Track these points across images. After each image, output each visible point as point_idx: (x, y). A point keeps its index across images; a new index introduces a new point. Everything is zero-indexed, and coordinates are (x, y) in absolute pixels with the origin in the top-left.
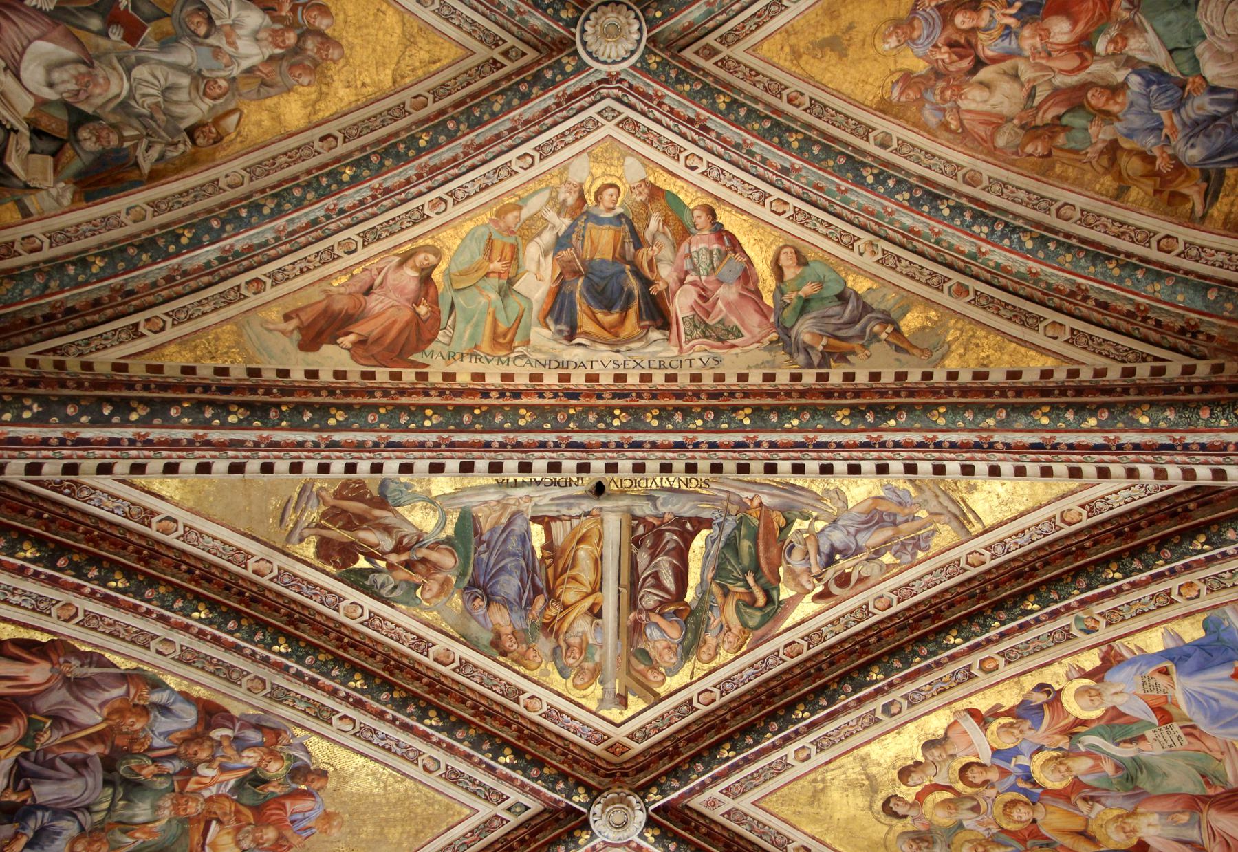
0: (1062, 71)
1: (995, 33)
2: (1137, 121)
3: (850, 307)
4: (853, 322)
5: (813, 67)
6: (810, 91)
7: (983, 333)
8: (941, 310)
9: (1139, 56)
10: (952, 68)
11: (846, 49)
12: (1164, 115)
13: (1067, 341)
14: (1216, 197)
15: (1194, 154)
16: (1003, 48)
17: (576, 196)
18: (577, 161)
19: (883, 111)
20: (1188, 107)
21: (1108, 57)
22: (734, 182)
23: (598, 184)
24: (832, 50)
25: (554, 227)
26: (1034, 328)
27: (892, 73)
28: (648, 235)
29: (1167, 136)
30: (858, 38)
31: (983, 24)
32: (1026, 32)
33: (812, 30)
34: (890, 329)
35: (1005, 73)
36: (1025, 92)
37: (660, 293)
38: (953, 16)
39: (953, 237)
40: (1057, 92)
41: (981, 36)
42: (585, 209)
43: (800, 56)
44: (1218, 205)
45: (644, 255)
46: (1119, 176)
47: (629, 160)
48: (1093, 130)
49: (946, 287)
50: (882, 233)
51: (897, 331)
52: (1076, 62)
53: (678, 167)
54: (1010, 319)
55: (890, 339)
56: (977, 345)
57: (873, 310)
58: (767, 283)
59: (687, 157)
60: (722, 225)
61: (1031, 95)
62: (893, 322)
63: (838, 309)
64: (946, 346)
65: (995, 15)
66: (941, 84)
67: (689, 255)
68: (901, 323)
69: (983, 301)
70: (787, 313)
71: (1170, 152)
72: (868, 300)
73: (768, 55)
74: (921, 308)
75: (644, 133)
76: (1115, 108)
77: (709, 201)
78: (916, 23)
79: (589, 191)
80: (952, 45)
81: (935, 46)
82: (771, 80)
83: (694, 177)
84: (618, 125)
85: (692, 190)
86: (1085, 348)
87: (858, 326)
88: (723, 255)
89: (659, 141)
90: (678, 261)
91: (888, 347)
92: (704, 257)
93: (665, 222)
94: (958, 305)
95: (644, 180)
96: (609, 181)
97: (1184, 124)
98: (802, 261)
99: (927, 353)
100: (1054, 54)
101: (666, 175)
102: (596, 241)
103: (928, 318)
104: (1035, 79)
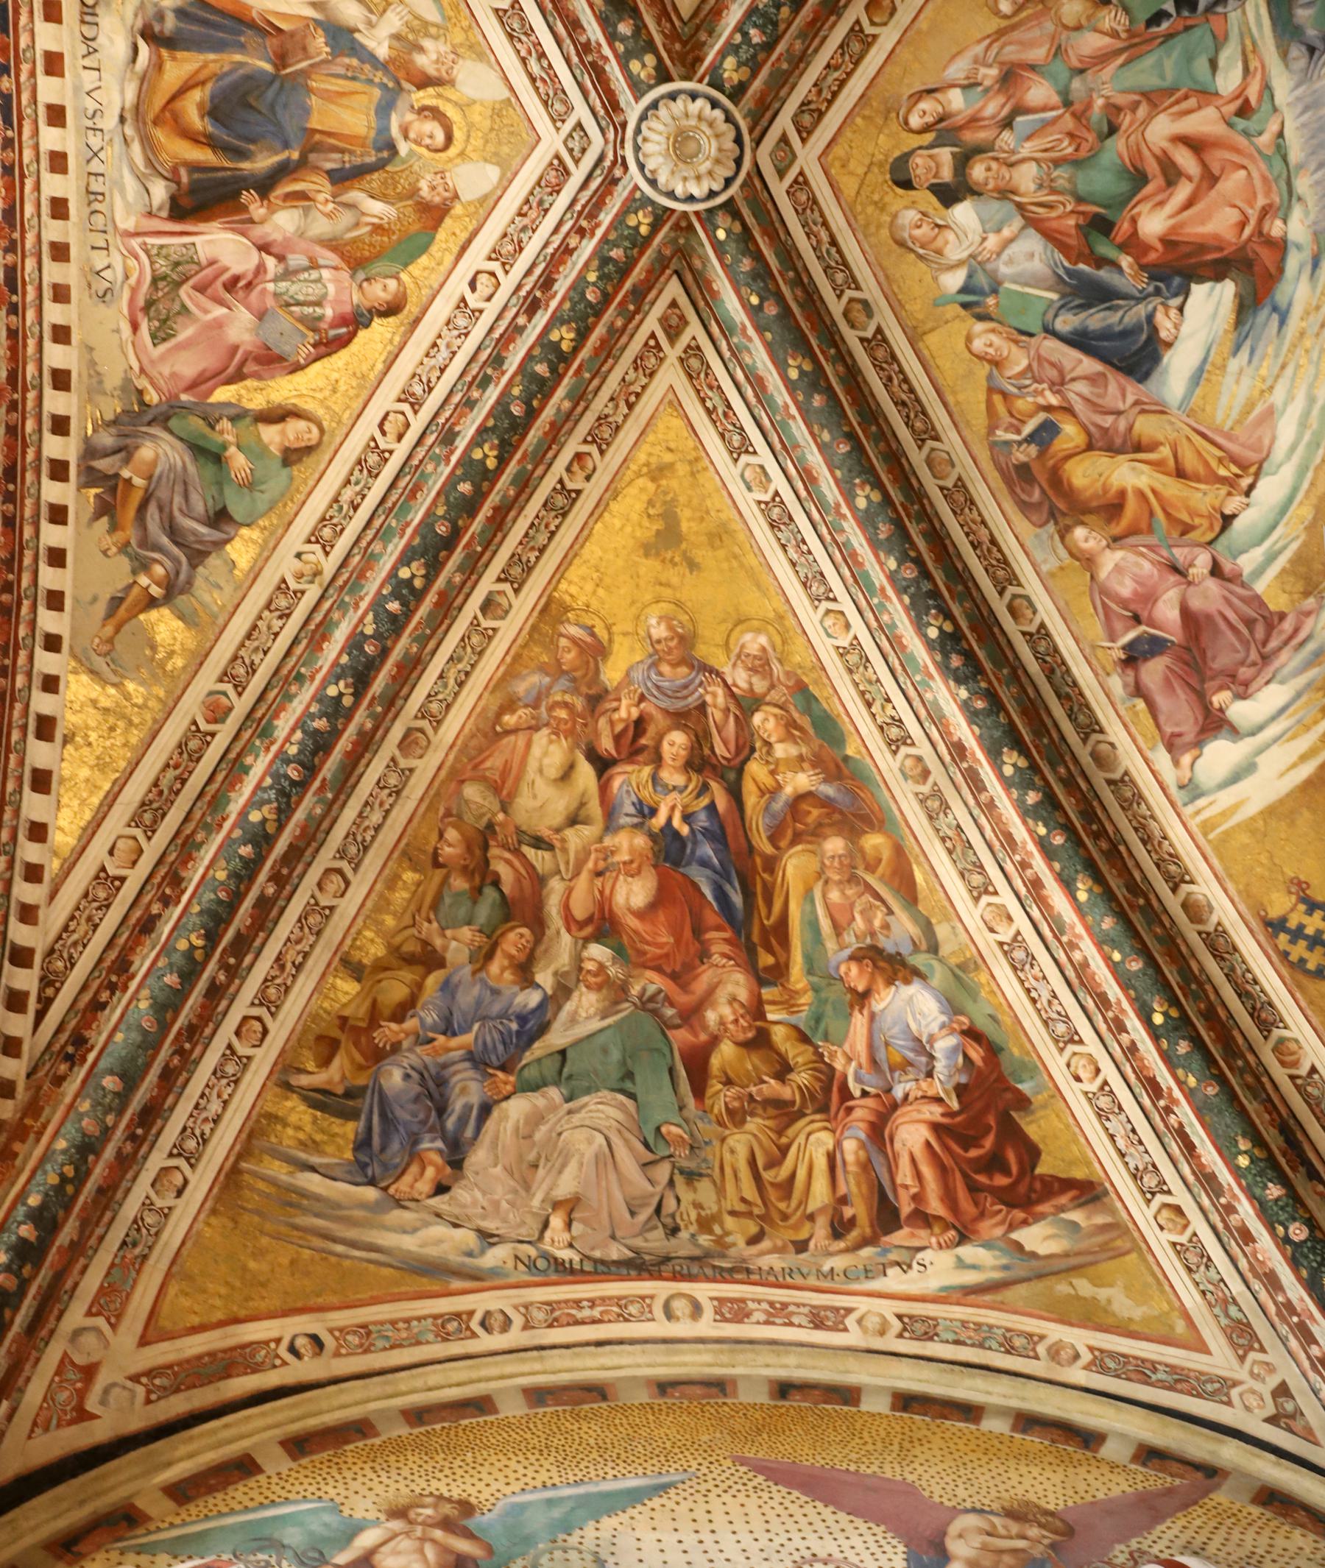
0: (570, 891)
1: (647, 794)
2: (466, 998)
3: (203, 530)
4: (173, 531)
5: (633, 501)
6: (592, 492)
7: (134, 740)
8: (184, 677)
9: (569, 1007)
10: (602, 722)
11: (658, 554)
12: (467, 1039)
13: (103, 869)
14: (314, 1105)
15: (394, 1078)
16: (622, 804)
17: (432, 71)
18: (493, 77)
19: (545, 609)
20: (471, 1073)
21: (578, 961)
22: (444, 353)
23: (451, 112)
24: (658, 532)
25: (371, 25)
26: (135, 820)
27: (608, 628)
28: (355, 195)
29: (433, 1040)
30: (672, 575)
31: (665, 775)
32: (641, 841)
33: (695, 502)
34: (156, 591)
35: (582, 805)
36: (545, 833)
37: (244, 209)
38: (684, 728)
39: (302, 699)
40: (539, 881)
41: (647, 770)
42: (406, 85)
43: (653, 479)
44: (302, 1107)
45: (318, 186)
46: (381, 967)
47: (493, 173)
48: (466, 933)
49: (228, 688)
50: (331, 591)
51: (152, 603)
52: (579, 912)
53: (476, 258)
54: (156, 784)
55: (136, 590)
56: (112, 729)
57: (193, 566)
58: (253, 395)
59: (493, 274)
60: (367, 326)
61: (539, 843)
62: (168, 598)
63: (199, 507)
64: (116, 680)
65: (675, 795)
66: (579, 703)
67: (314, 265)
68: (165, 611)
69: (194, 744)
70: (196, 423)
71: (405, 1044)
72: (213, 561)
73: (661, 426)
74: (191, 644)
75: (541, 203)
76: (495, 967)
77: (411, 309)
78: (683, 670)
79: (439, 96)
80: (640, 725)
81: (642, 698)
82: (618, 428)
83: (457, 285)
84: (557, 156)
85: (435, 281)
86: (86, 895)
87: (165, 541)
88: (312, 324)
89: (524, 229)
90: (303, 245)
91: (121, 585)
92: (312, 292)
93: (378, 229)
94: (191, 705)
95: (456, 196)
96: (458, 134)
97: (445, 1066)
98: (292, 456)
99: (105, 648)
100: (598, 882)
101: (464, 236)
102: (344, 101)
103: (171, 654)
104: (565, 850)
